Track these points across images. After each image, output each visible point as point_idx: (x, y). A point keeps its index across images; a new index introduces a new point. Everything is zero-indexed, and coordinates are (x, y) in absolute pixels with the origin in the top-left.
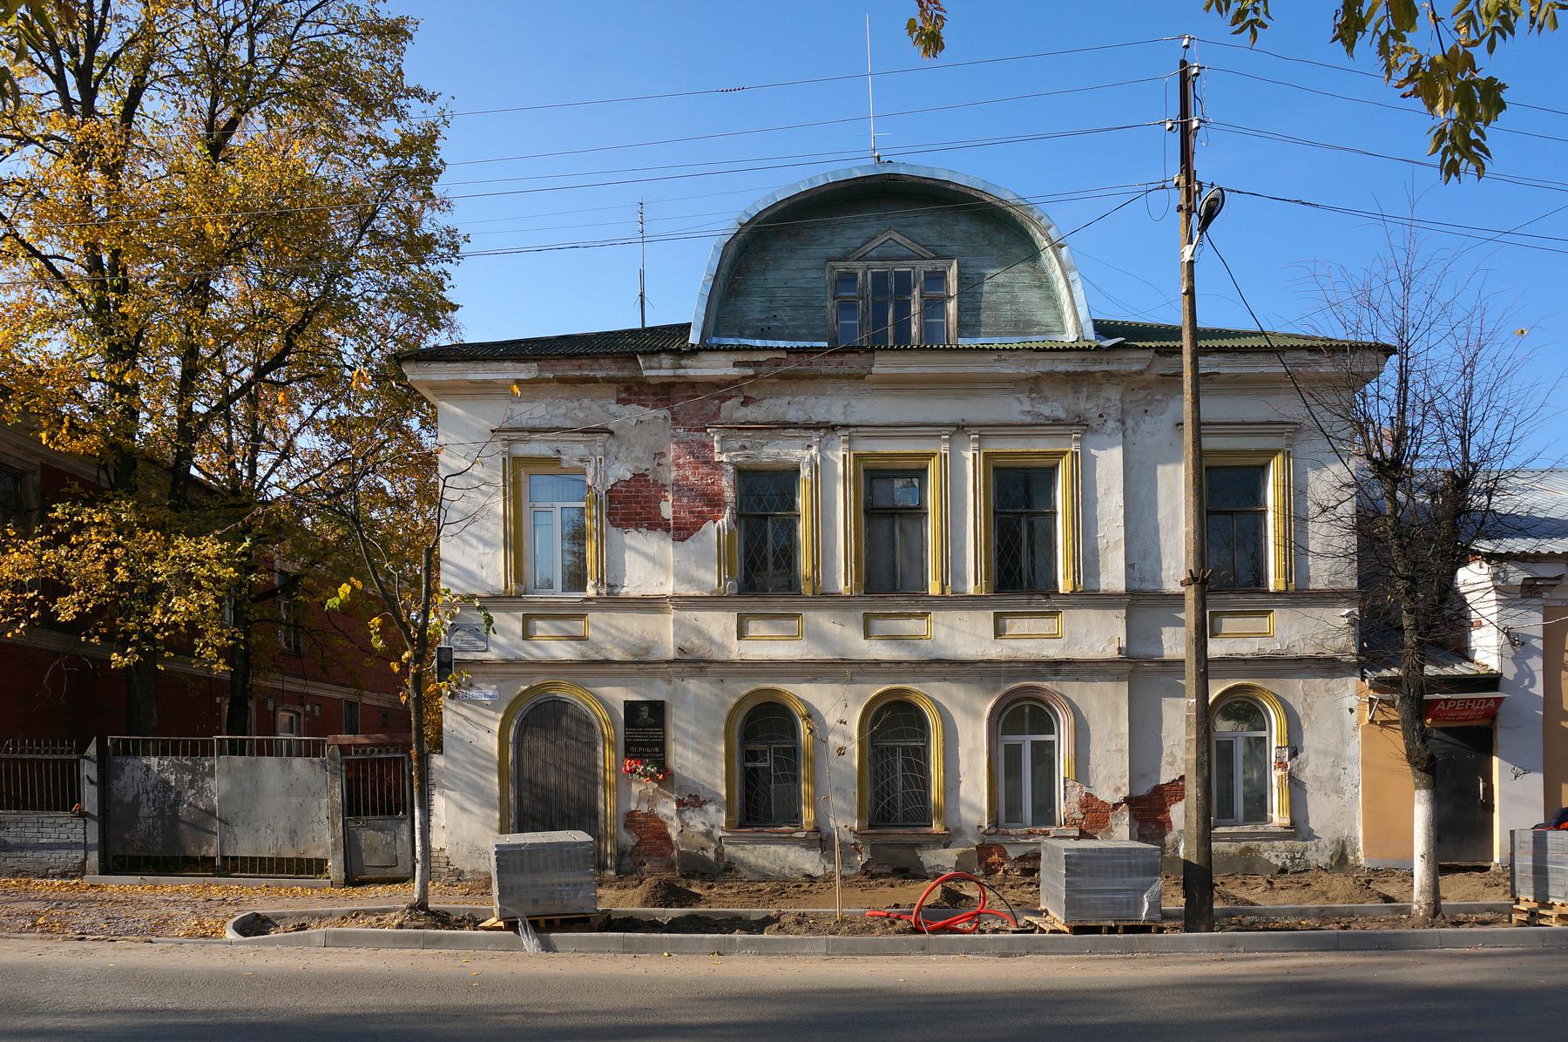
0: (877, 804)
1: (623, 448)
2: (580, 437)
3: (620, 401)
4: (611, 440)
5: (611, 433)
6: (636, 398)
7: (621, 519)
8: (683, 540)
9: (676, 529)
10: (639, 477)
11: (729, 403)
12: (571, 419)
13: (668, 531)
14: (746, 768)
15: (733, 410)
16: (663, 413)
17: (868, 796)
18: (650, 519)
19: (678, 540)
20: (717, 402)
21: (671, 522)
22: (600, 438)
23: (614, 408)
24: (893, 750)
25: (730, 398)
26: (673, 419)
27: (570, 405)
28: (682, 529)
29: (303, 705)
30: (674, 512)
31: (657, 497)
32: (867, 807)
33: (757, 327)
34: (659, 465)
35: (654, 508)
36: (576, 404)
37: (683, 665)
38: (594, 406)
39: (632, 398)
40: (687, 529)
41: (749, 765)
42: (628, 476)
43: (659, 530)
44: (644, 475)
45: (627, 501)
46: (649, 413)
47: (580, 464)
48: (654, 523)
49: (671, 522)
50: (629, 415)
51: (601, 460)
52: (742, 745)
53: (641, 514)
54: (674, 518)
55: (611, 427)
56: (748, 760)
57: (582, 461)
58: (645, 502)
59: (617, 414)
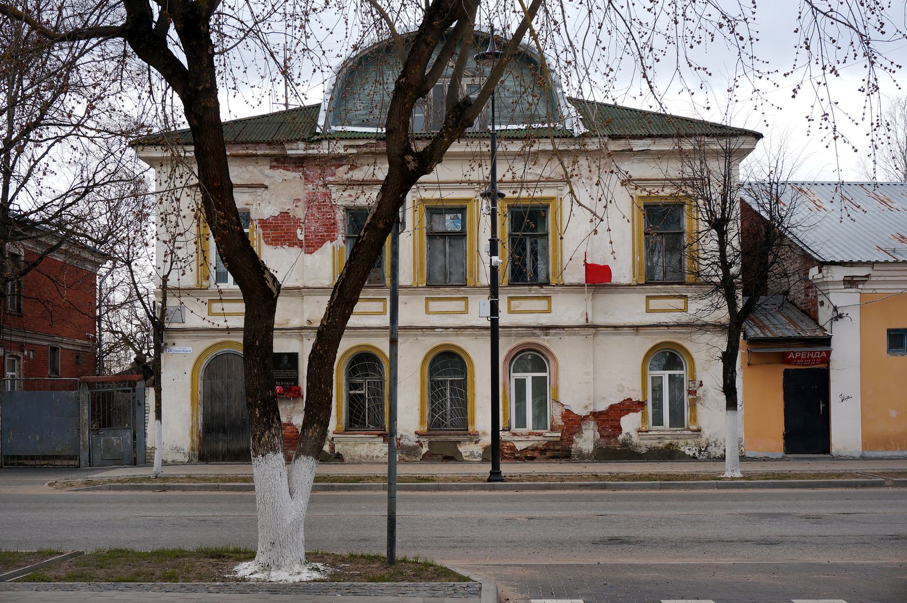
0: (433, 417)
1: (274, 197)
2: (246, 190)
3: (272, 167)
4: (266, 191)
5: (266, 187)
6: (283, 165)
7: (272, 240)
8: (311, 253)
9: (307, 246)
10: (285, 215)
11: (341, 169)
12: (241, 178)
13: (301, 247)
14: (350, 394)
15: (342, 173)
16: (298, 175)
17: (427, 411)
18: (290, 240)
19: (308, 253)
20: (333, 168)
21: (304, 242)
22: (260, 191)
23: (268, 171)
24: (443, 383)
25: (342, 165)
26: (305, 179)
27: (240, 170)
28: (310, 246)
29: (23, 351)
30: (305, 236)
31: (295, 226)
32: (427, 419)
33: (360, 119)
34: (296, 206)
35: (294, 233)
36: (244, 169)
37: (310, 331)
38: (256, 170)
39: (280, 165)
40: (314, 246)
41: (352, 392)
42: (277, 214)
43: (296, 246)
44: (287, 213)
45: (276, 228)
46: (290, 175)
47: (246, 206)
48: (293, 242)
49: (304, 242)
50: (279, 174)
51: (259, 204)
52: (347, 380)
53: (284, 237)
54: (305, 239)
55: (266, 183)
56: (351, 389)
57: (247, 204)
58: (287, 230)
59: (270, 175)
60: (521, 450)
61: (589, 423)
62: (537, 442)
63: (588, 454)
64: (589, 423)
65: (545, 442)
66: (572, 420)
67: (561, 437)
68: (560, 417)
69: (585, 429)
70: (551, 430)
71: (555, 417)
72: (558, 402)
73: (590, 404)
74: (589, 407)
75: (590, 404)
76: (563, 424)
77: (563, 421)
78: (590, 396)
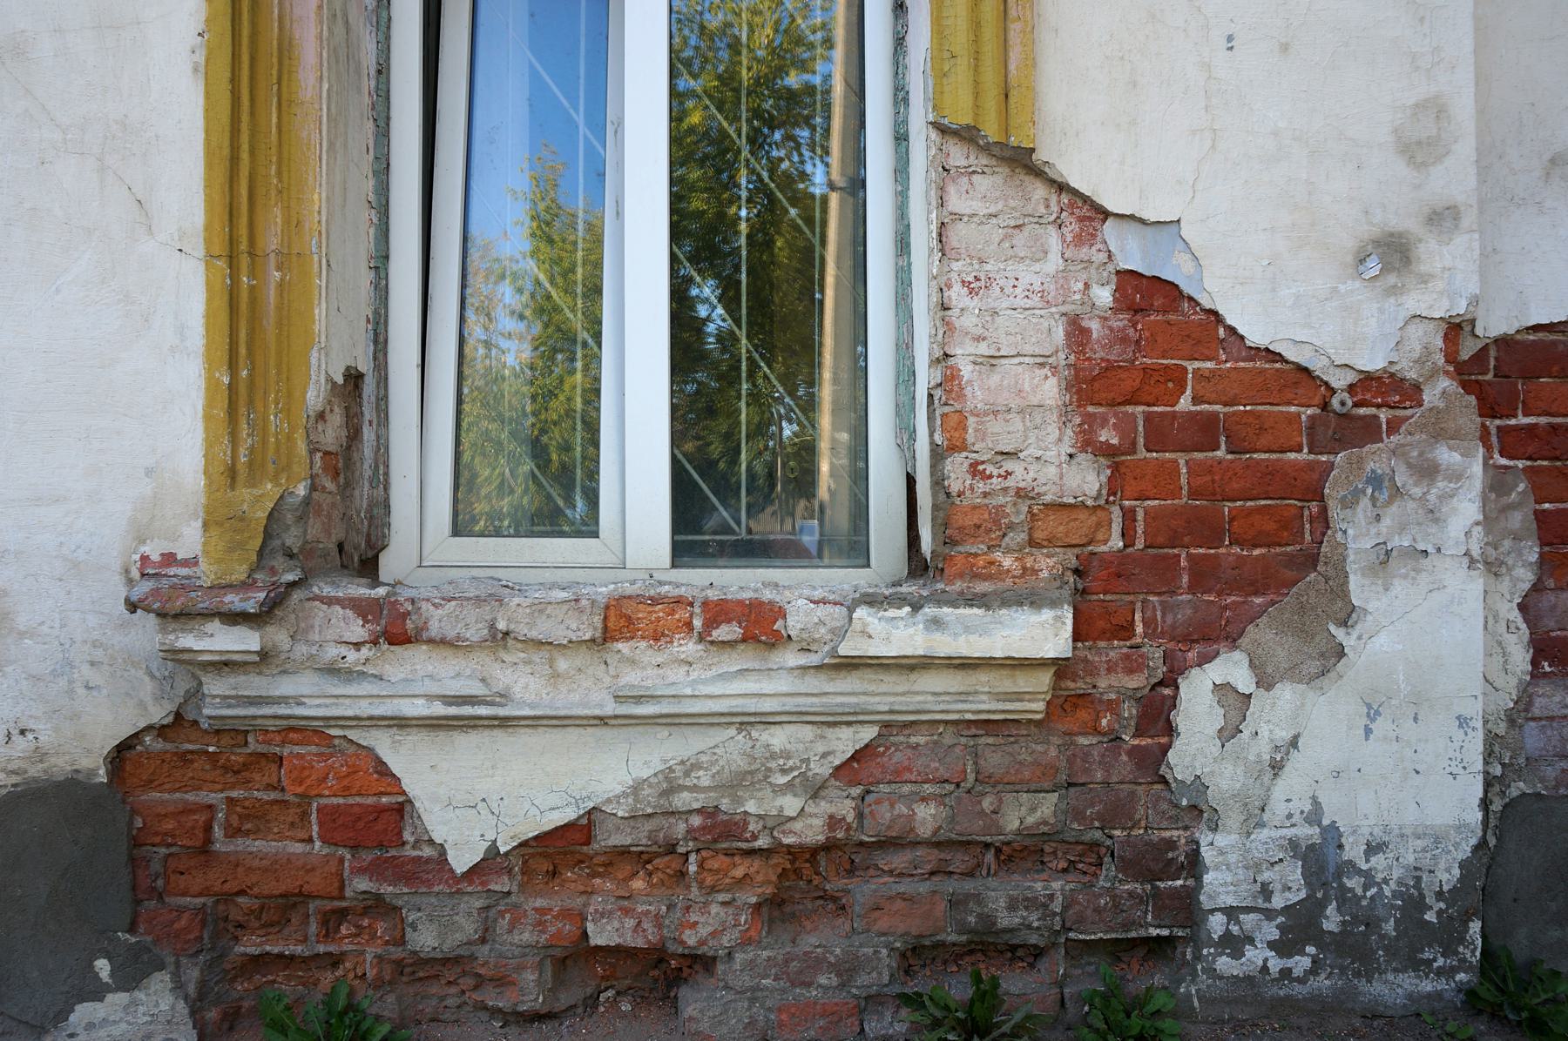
60: (491, 862)
61: (1428, 471)
62: (731, 748)
63: (1413, 903)
64: (1428, 471)
65: (845, 742)
66: (1204, 431)
67: (1061, 668)
68: (1049, 390)
69: (1384, 558)
70: (918, 566)
71: (976, 395)
72: (1037, 172)
73: (1442, 218)
74: (1437, 255)
75: (1442, 218)
76: (1087, 480)
77: (1087, 443)
78: (1436, 108)
